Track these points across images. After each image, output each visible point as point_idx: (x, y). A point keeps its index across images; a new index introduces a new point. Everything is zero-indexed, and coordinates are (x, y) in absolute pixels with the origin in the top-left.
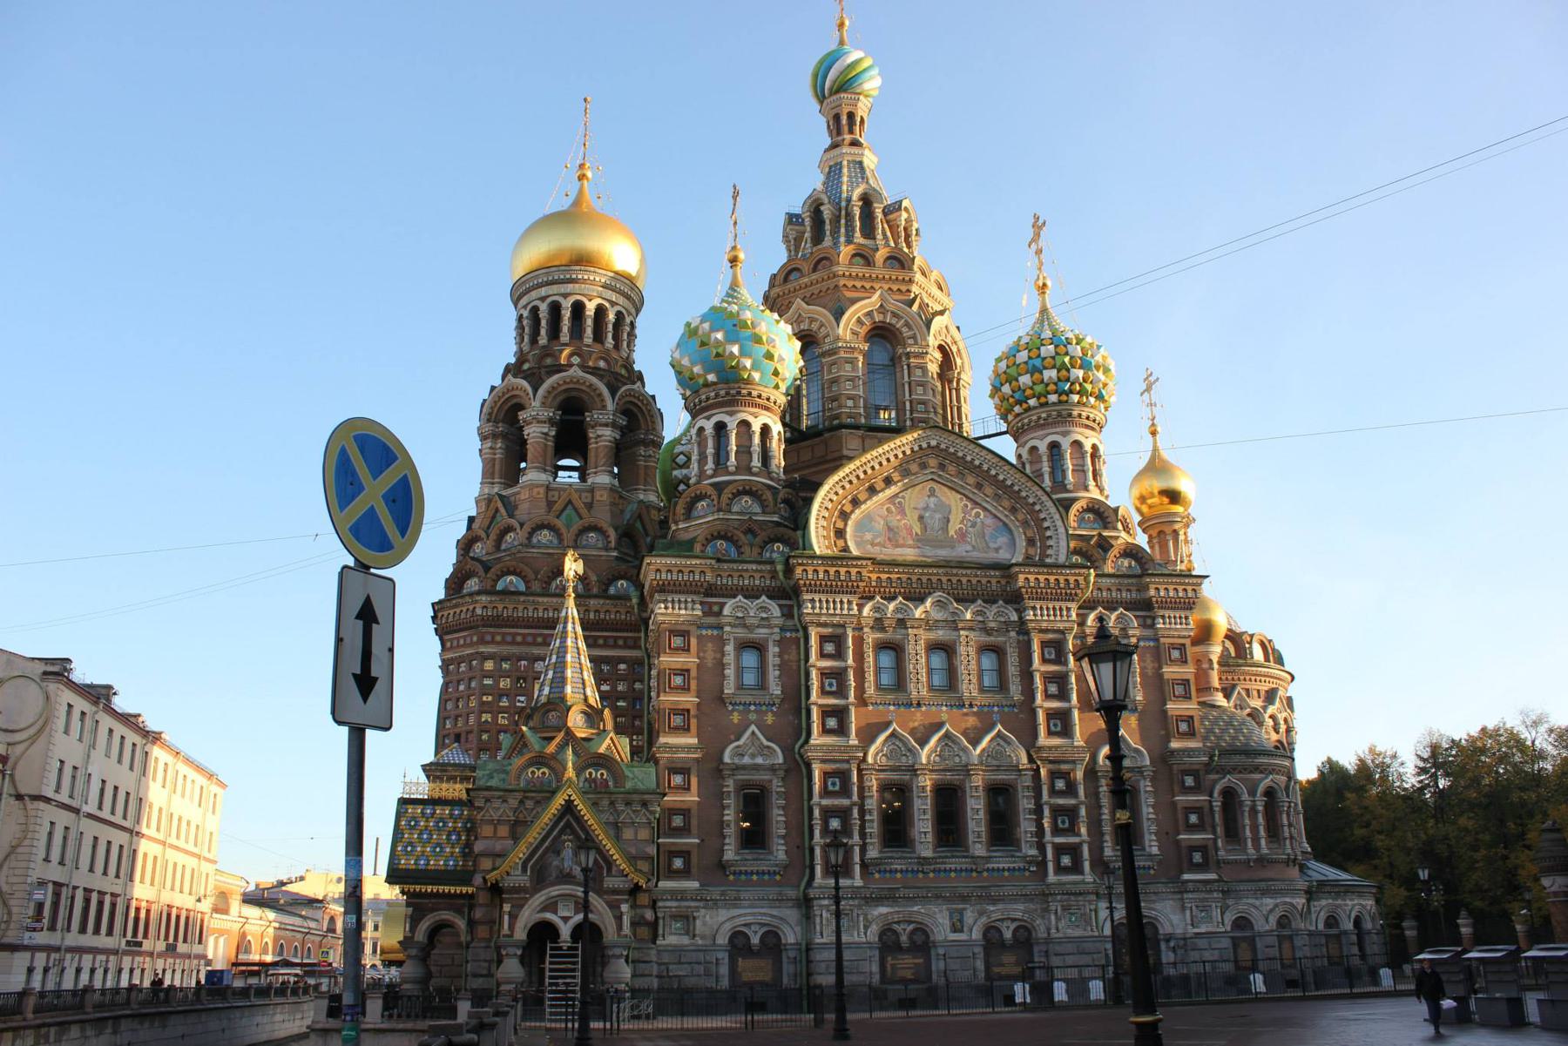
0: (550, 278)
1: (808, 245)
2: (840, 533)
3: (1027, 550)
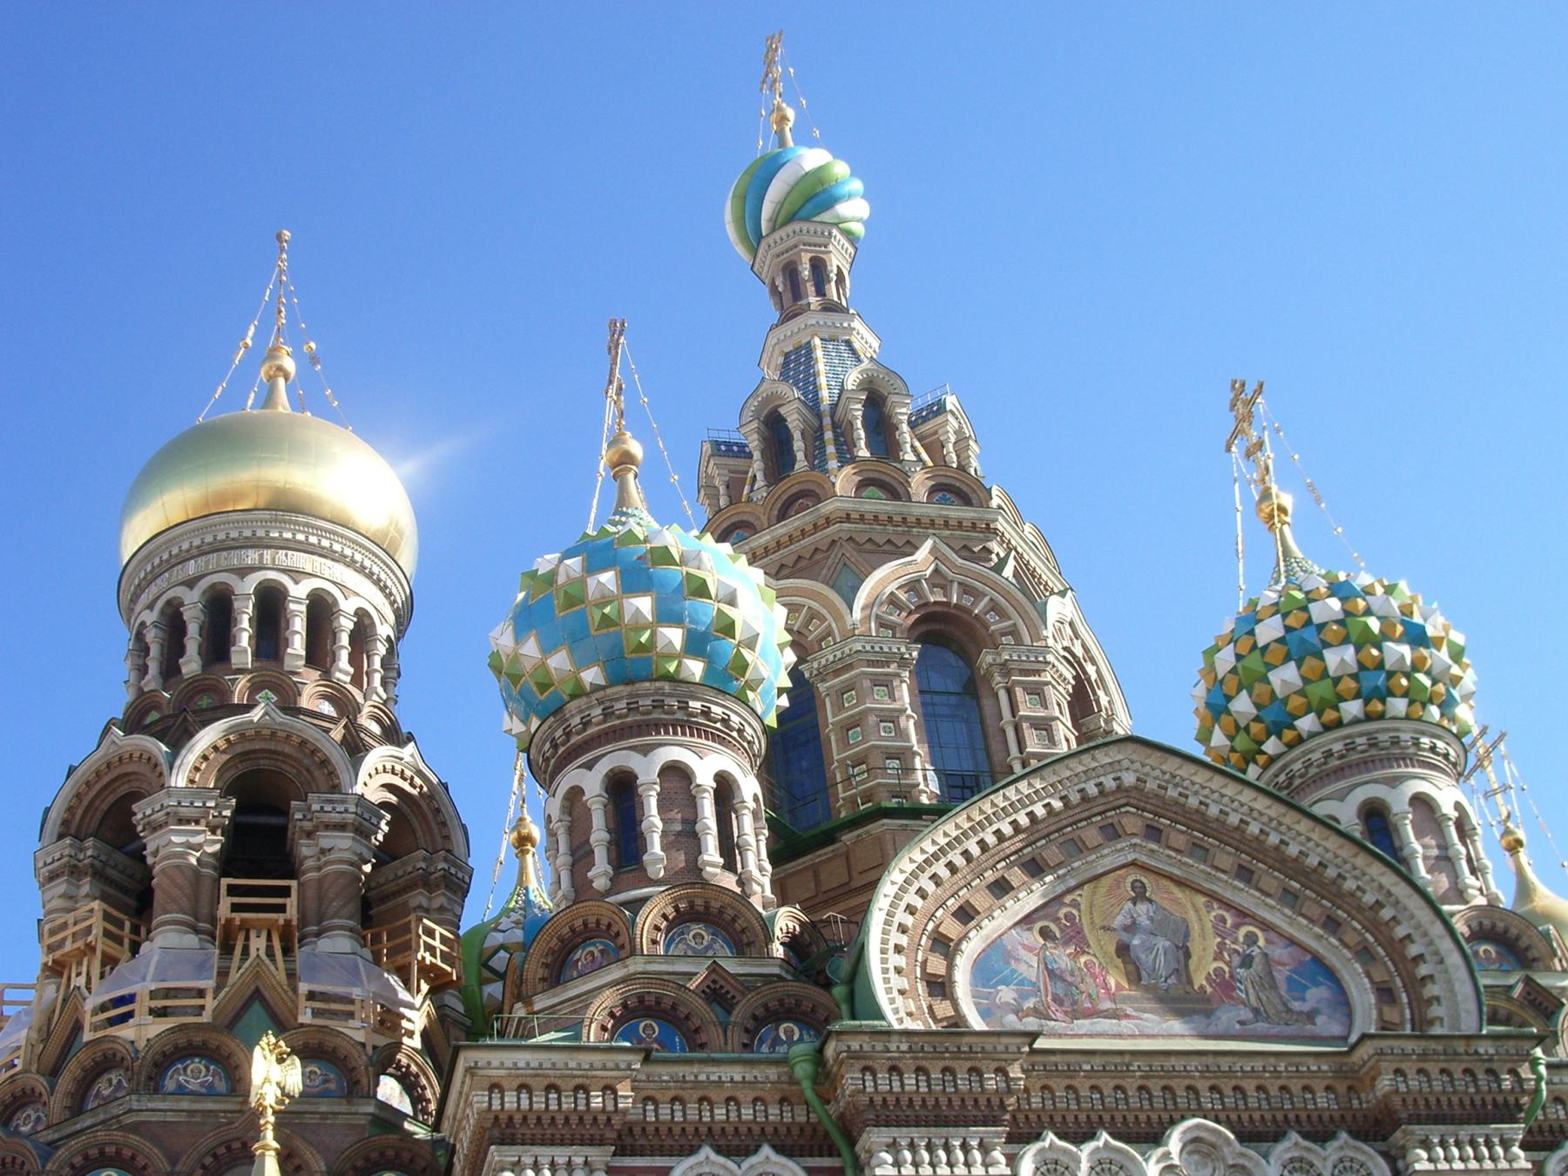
0: (209, 539)
1: (760, 483)
2: (940, 987)
3: (1380, 1014)
